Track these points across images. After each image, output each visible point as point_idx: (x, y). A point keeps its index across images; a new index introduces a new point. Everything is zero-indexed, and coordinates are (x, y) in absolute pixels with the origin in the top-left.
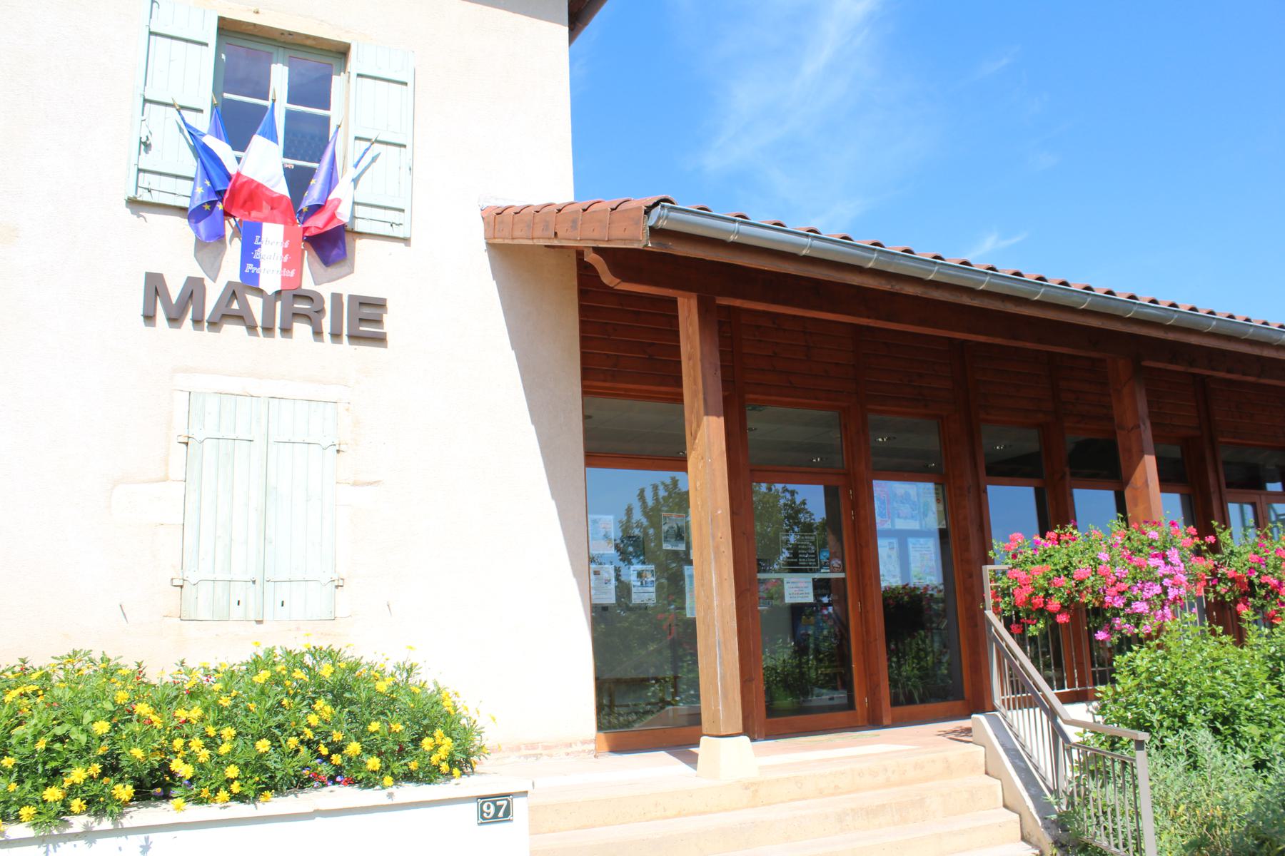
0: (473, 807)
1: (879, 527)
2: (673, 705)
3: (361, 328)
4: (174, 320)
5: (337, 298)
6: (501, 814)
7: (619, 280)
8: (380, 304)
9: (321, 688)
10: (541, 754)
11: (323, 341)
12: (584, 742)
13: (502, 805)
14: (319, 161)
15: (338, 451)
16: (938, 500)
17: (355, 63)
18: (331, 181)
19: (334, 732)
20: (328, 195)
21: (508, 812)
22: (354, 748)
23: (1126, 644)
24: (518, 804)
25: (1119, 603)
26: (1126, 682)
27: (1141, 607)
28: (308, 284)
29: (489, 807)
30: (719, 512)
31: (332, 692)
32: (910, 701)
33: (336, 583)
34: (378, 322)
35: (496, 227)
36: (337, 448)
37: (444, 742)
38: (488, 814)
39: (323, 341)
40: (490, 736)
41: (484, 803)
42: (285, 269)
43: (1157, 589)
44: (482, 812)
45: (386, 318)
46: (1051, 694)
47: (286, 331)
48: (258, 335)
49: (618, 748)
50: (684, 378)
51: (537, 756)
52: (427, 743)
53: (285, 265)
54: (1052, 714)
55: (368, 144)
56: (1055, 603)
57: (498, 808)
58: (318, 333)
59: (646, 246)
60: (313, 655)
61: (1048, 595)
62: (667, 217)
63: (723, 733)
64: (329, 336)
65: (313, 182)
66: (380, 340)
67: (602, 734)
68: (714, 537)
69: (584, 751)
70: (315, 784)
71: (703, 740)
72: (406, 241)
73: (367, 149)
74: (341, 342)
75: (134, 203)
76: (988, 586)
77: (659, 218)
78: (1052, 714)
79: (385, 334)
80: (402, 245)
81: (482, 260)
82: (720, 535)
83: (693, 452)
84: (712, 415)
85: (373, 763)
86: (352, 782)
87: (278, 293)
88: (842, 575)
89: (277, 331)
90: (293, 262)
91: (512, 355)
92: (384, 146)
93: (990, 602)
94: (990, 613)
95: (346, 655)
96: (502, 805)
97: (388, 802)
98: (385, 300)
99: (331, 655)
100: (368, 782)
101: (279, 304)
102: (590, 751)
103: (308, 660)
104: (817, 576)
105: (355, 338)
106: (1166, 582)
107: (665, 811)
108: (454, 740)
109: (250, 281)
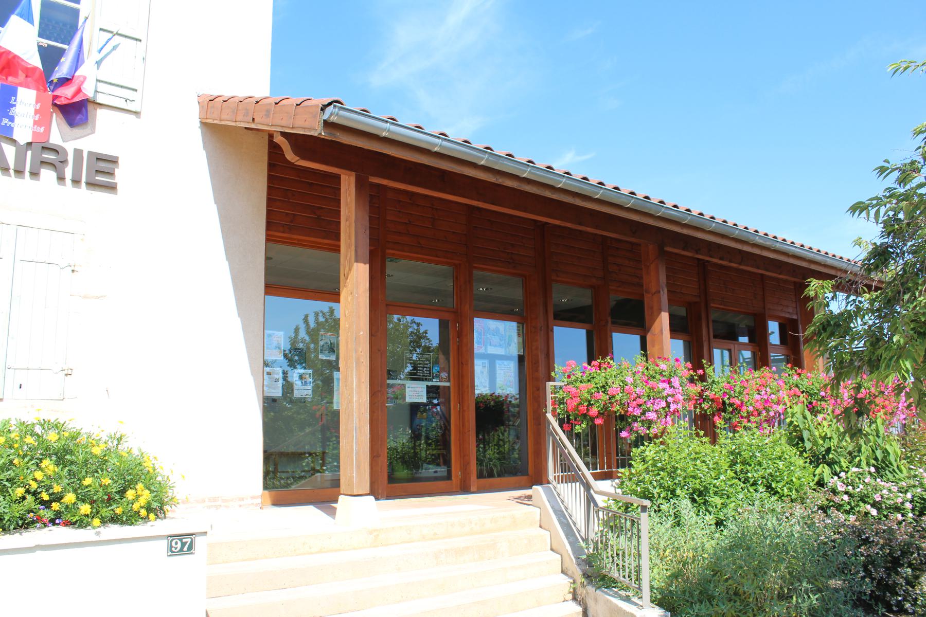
0: (164, 543)
1: (476, 351)
2: (321, 473)
3: (97, 178)
5: (78, 153)
6: (186, 549)
7: (298, 158)
8: (114, 161)
9: (48, 452)
10: (220, 506)
11: (64, 185)
12: (253, 498)
13: (187, 542)
14: (69, 44)
15: (73, 271)
16: (519, 335)
18: (78, 60)
19: (55, 485)
20: (76, 69)
21: (191, 547)
22: (70, 498)
23: (640, 441)
24: (199, 541)
25: (637, 412)
26: (638, 466)
27: (652, 415)
28: (55, 138)
29: (176, 543)
30: (361, 333)
31: (56, 454)
32: (491, 475)
33: (66, 372)
34: (111, 174)
35: (209, 110)
36: (72, 268)
37: (143, 493)
38: (176, 548)
39: (64, 185)
40: (179, 490)
41: (172, 540)
42: (36, 126)
43: (663, 404)
44: (171, 547)
45: (117, 172)
46: (588, 473)
47: (35, 174)
48: (10, 176)
49: (278, 502)
50: (342, 234)
51: (217, 507)
52: (130, 494)
53: (35, 123)
54: (587, 487)
55: (110, 35)
56: (594, 410)
57: (183, 544)
58: (61, 179)
59: (320, 134)
60: (42, 425)
61: (590, 405)
62: (337, 114)
63: (355, 494)
64: (70, 182)
65: (63, 59)
66: (111, 188)
67: (266, 492)
68: (356, 351)
69: (253, 504)
70: (38, 525)
71: (341, 498)
72: (137, 114)
73: (110, 39)
74: (80, 187)
76: (549, 396)
77: (331, 114)
78: (587, 487)
79: (116, 183)
80: (133, 117)
81: (196, 134)
82: (360, 350)
83: (345, 289)
84: (361, 262)
85: (85, 509)
86: (68, 524)
87: (29, 144)
88: (447, 384)
89: (27, 174)
90: (42, 121)
91: (214, 208)
92: (124, 39)
93: (550, 407)
94: (549, 416)
95: (69, 427)
96: (187, 542)
97: (96, 538)
98: (118, 158)
99: (57, 426)
100: (81, 524)
101: (29, 153)
102: (257, 505)
103: (38, 429)
104: (430, 384)
105: (91, 185)
106: (670, 399)
107: (310, 548)
108: (152, 492)
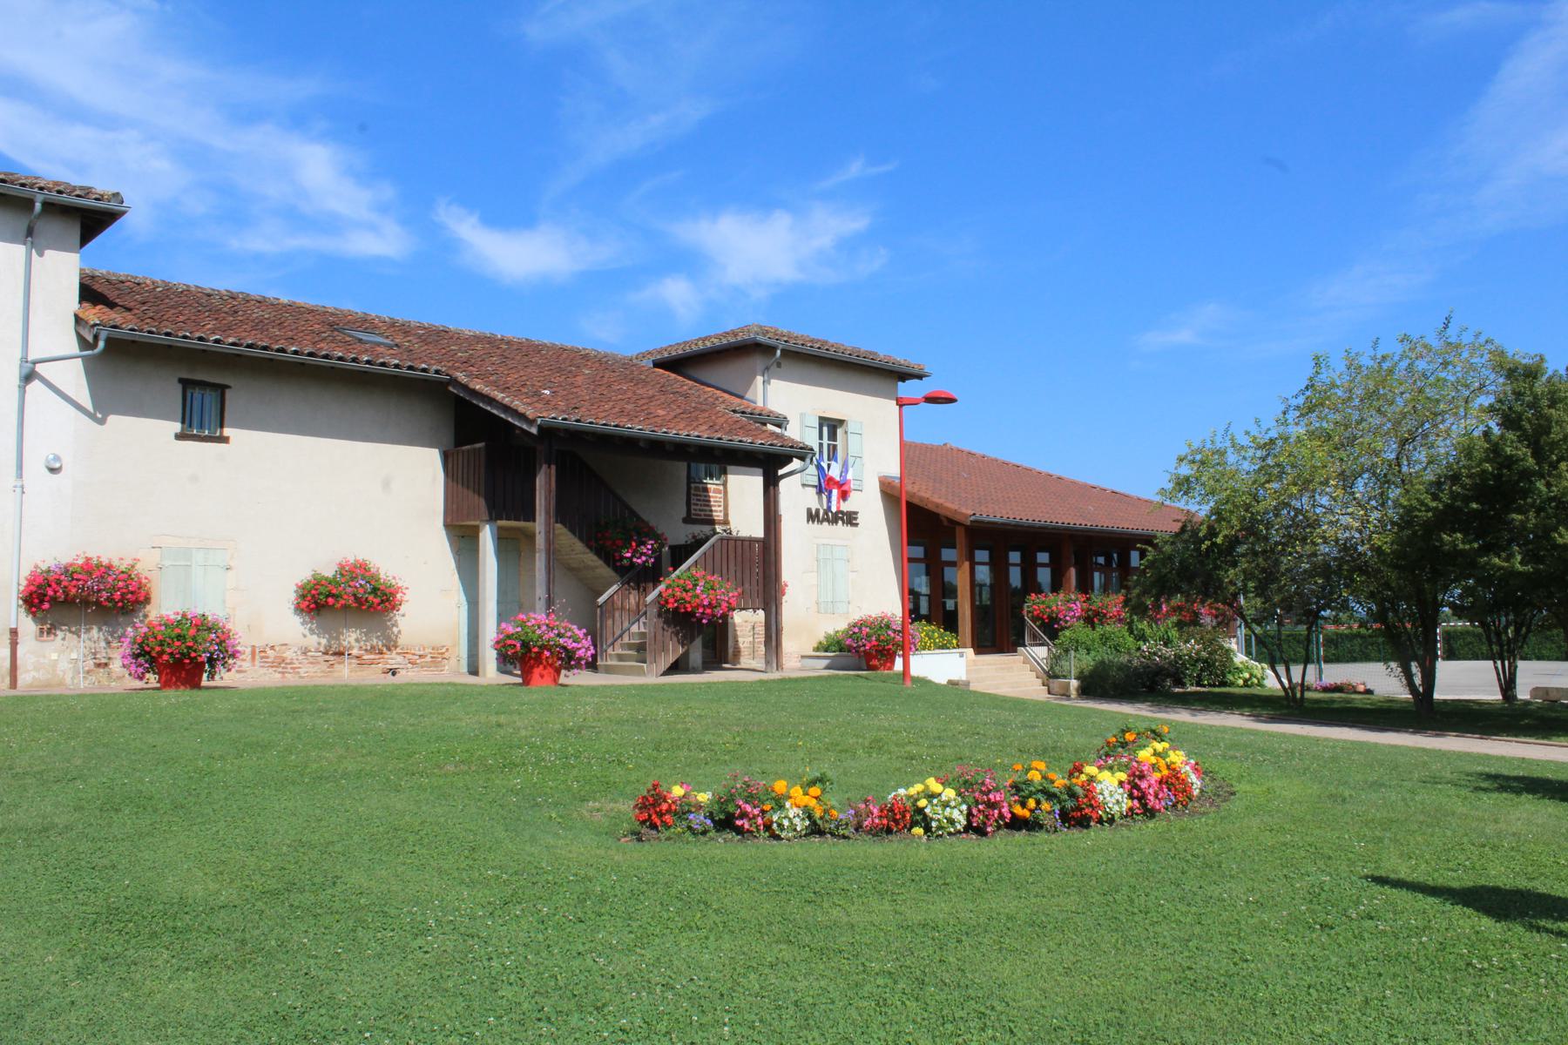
4: (813, 522)
8: (856, 513)
17: (851, 427)
23: (1063, 629)
27: (1068, 618)
47: (837, 523)
58: (843, 523)
66: (857, 525)
75: (804, 485)
76: (1026, 609)
81: (878, 495)
90: (838, 502)
109: (829, 507)
